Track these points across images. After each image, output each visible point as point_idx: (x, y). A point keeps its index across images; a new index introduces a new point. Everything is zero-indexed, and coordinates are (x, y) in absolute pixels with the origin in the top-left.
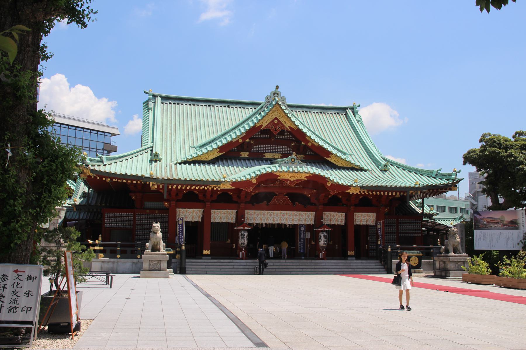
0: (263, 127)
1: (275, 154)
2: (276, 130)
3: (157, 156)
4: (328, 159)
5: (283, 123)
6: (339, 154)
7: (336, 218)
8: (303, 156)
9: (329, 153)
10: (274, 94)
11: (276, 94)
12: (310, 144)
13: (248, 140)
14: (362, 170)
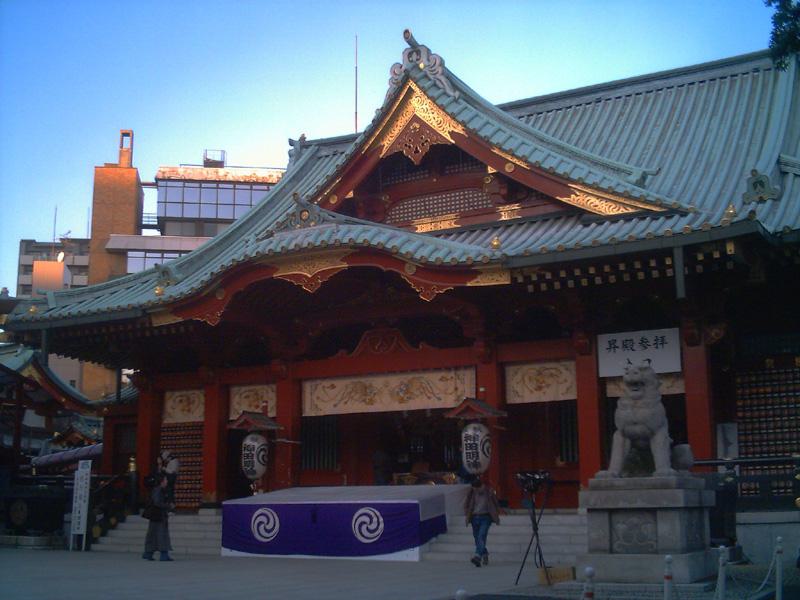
0: (384, 152)
1: (439, 218)
2: (417, 151)
3: (167, 273)
4: (564, 200)
5: (434, 125)
6: (597, 176)
7: (541, 384)
8: (516, 207)
9: (564, 182)
10: (410, 55)
11: (415, 49)
12: (508, 169)
13: (351, 195)
14: (671, 212)
